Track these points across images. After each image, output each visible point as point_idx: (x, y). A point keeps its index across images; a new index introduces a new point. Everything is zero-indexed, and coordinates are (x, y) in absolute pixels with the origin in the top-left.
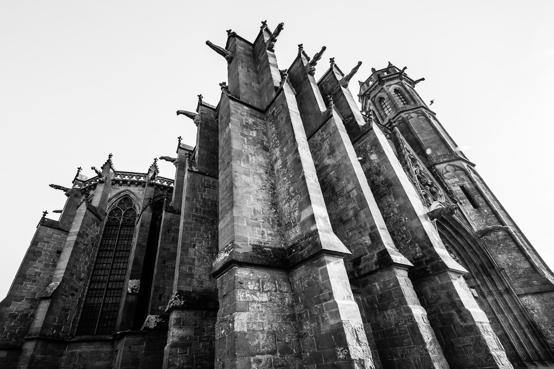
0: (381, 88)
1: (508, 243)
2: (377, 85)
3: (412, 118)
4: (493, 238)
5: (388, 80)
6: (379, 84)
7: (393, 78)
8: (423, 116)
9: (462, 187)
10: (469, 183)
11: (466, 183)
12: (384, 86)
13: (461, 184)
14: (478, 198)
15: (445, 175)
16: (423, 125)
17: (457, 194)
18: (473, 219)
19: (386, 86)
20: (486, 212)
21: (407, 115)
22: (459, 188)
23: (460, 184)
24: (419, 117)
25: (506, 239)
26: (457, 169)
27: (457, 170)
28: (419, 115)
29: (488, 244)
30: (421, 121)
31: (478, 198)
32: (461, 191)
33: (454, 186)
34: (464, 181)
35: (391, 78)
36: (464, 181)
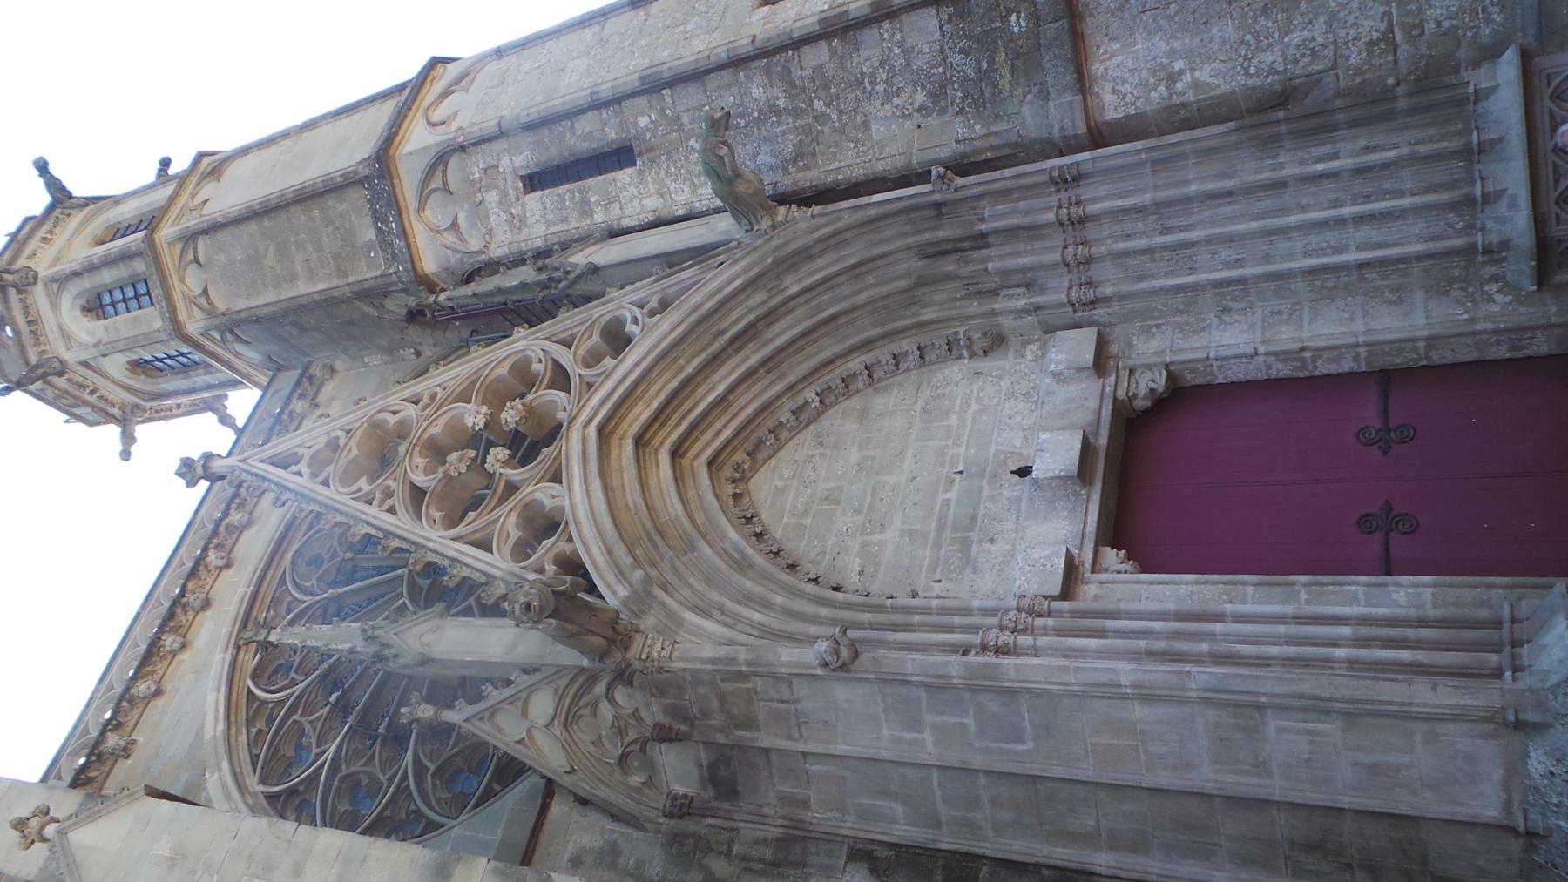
0: (83, 370)
1: (808, 72)
2: (69, 380)
3: (205, 292)
4: (784, 133)
6: (61, 374)
8: (195, 243)
9: (534, 181)
10: (508, 151)
15: (474, 244)
16: (239, 255)
17: (562, 222)
20: (651, 121)
21: (197, 313)
22: (534, 200)
25: (786, 74)
26: (436, 182)
27: (445, 182)
28: (191, 256)
29: (816, 166)
30: (222, 258)
31: (579, 132)
32: (549, 196)
33: (523, 220)
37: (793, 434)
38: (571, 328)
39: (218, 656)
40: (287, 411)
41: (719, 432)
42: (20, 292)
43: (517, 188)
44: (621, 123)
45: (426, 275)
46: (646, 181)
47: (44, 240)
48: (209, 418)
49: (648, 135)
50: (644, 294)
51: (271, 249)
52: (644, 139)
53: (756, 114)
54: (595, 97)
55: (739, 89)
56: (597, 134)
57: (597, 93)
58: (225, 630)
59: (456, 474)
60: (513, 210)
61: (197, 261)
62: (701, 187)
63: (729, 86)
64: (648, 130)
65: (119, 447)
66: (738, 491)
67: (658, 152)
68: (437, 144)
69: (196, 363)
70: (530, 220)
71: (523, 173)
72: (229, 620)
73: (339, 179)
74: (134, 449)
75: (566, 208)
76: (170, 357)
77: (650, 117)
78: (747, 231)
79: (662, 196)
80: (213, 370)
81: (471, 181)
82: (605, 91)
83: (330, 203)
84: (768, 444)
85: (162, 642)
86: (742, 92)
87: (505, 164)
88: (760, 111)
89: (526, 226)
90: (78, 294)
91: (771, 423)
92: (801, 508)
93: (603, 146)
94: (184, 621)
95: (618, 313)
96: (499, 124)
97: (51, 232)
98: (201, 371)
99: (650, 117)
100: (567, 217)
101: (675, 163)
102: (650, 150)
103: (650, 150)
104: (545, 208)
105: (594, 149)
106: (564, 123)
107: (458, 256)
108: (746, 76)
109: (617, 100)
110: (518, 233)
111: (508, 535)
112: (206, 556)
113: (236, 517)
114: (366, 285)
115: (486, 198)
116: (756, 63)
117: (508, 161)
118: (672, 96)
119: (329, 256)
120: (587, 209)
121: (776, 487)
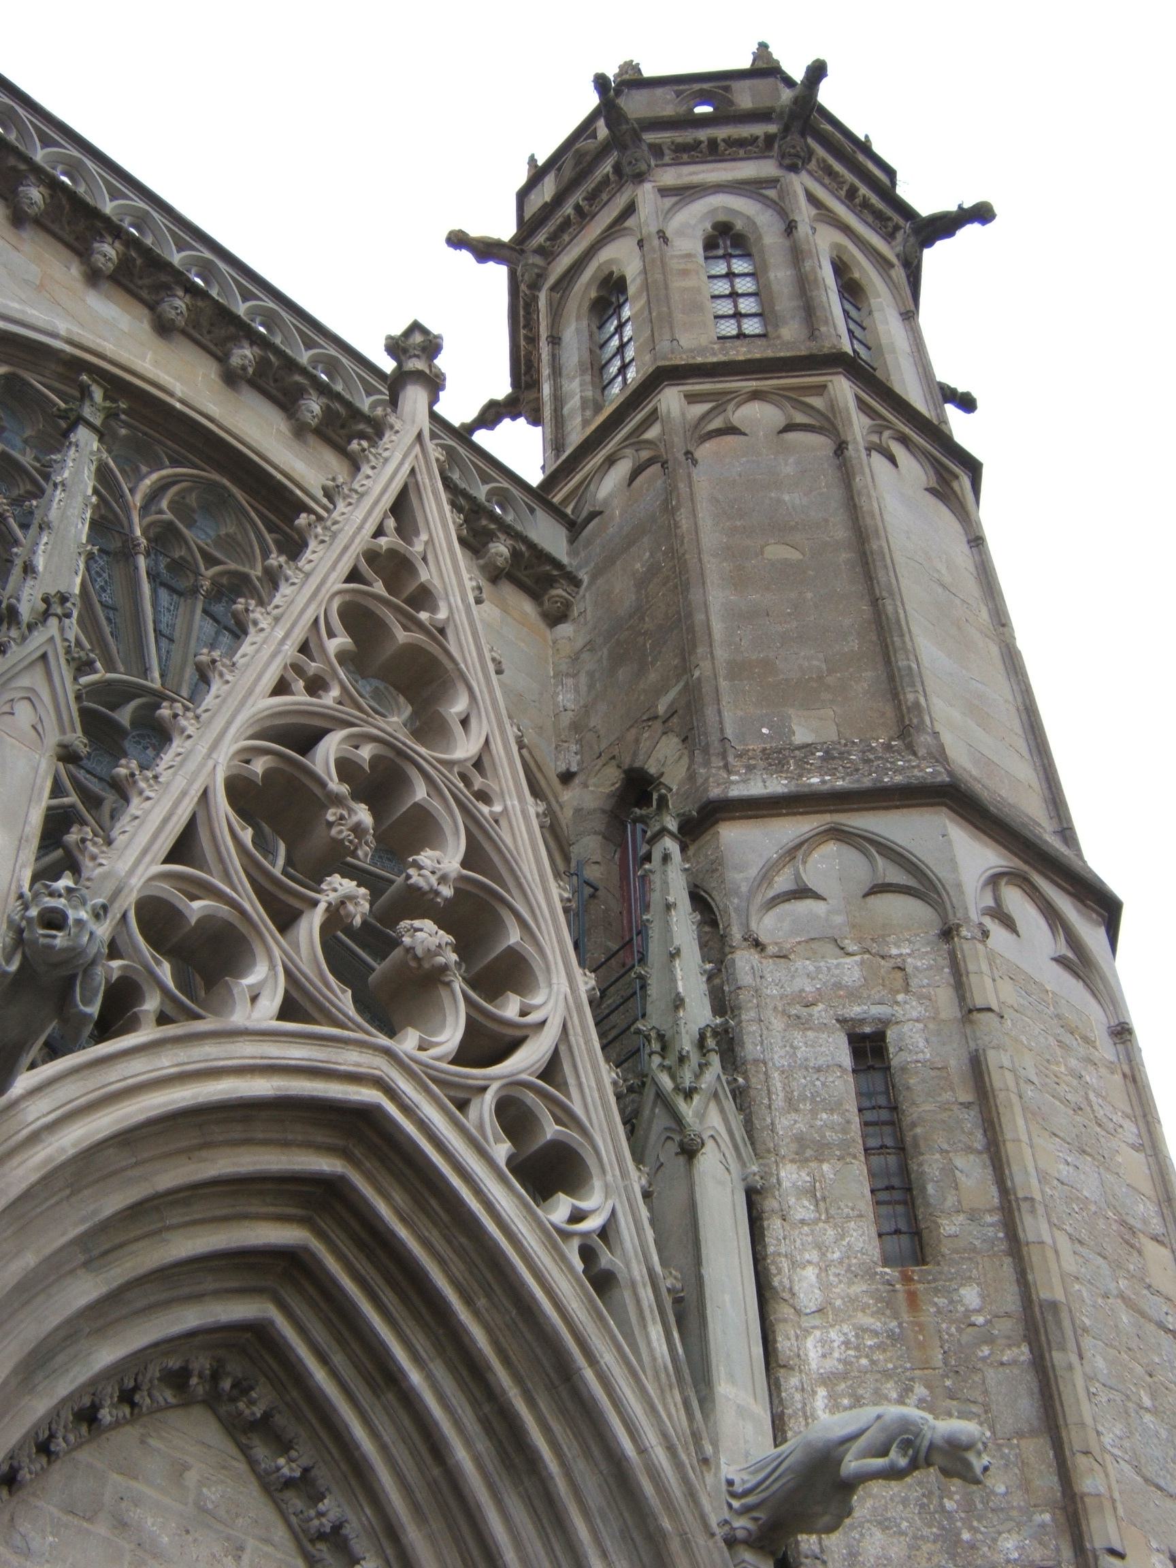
5: (688, 153)
7: (731, 142)
11: (911, 1008)
12: (646, 195)
13: (864, 1010)
14: (960, 1161)
17: (789, 1100)
18: (832, 1364)
19: (664, 192)
20: (968, 1313)
23: (855, 1010)
24: (791, 436)
31: (960, 1161)
34: (907, 989)
35: (713, 143)
36: (907, 989)
37: (294, 1519)
38: (580, 1085)
39: (62, 327)
40: (493, 526)
41: (323, 1359)
42: (770, 140)
43: (862, 1021)
44: (974, 1250)
45: (716, 822)
46: (850, 1283)
47: (852, 193)
48: (502, 388)
49: (942, 1301)
50: (628, 1245)
51: (795, 555)
52: (937, 1291)
53: (966, 1536)
54: (1025, 1206)
55: (1020, 1509)
56: (951, 1201)
57: (1033, 1211)
58: (108, 348)
59: (331, 818)
60: (821, 1006)
61: (790, 427)
62: (830, 1397)
63: (1025, 1485)
64: (951, 1302)
65: (474, 232)
66: (194, 1381)
67: (906, 1317)
68: (959, 885)
69: (604, 388)
70: (798, 1038)
71: (891, 1035)
72: (124, 356)
73: (911, 697)
74: (465, 256)
75: (814, 1113)
76: (622, 347)
77: (978, 1311)
78: (730, 1483)
79: (819, 1311)
80: (588, 413)
81: (883, 936)
82: (1034, 1227)
83: (868, 674)
84: (281, 1461)
85: (110, 240)
86: (1014, 1513)
87: (911, 1008)
88: (973, 1547)
89: (788, 1026)
90: (754, 223)
91: (323, 1476)
92: (134, 1514)
93: (928, 1205)
94: (140, 282)
95: (597, 1183)
96: (990, 1010)
97: (865, 204)
98: (589, 394)
99: (978, 1311)
100: (797, 1110)
101: (881, 1347)
102: (913, 1300)
103: (913, 1300)
104: (818, 1070)
105: (923, 1189)
106: (979, 1135)
107: (744, 889)
108: (1043, 1526)
109: (1015, 1246)
110: (775, 1008)
111: (193, 898)
112: (252, 343)
113: (314, 406)
114: (710, 712)
115: (849, 960)
116: (1067, 1553)
117: (915, 1014)
118: (1014, 1362)
119: (771, 655)
120: (809, 1153)
121: (186, 1467)
